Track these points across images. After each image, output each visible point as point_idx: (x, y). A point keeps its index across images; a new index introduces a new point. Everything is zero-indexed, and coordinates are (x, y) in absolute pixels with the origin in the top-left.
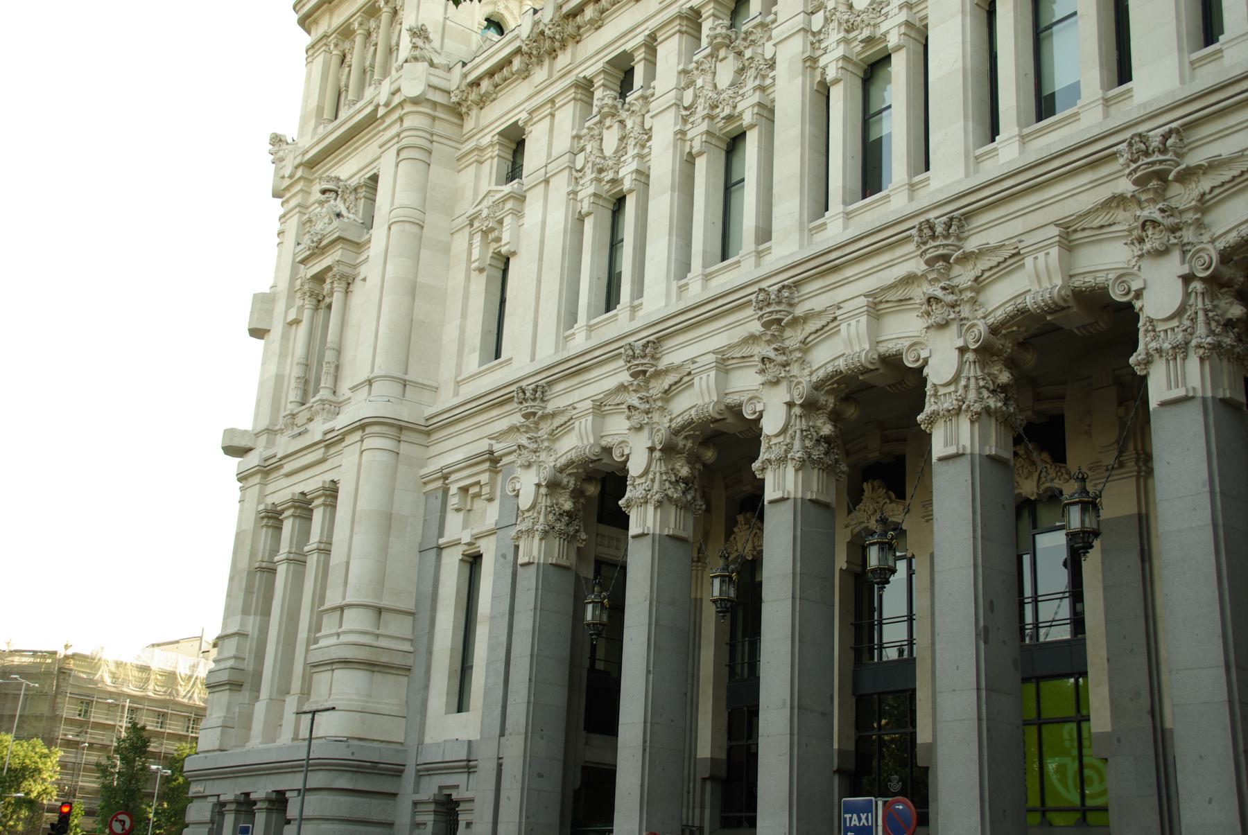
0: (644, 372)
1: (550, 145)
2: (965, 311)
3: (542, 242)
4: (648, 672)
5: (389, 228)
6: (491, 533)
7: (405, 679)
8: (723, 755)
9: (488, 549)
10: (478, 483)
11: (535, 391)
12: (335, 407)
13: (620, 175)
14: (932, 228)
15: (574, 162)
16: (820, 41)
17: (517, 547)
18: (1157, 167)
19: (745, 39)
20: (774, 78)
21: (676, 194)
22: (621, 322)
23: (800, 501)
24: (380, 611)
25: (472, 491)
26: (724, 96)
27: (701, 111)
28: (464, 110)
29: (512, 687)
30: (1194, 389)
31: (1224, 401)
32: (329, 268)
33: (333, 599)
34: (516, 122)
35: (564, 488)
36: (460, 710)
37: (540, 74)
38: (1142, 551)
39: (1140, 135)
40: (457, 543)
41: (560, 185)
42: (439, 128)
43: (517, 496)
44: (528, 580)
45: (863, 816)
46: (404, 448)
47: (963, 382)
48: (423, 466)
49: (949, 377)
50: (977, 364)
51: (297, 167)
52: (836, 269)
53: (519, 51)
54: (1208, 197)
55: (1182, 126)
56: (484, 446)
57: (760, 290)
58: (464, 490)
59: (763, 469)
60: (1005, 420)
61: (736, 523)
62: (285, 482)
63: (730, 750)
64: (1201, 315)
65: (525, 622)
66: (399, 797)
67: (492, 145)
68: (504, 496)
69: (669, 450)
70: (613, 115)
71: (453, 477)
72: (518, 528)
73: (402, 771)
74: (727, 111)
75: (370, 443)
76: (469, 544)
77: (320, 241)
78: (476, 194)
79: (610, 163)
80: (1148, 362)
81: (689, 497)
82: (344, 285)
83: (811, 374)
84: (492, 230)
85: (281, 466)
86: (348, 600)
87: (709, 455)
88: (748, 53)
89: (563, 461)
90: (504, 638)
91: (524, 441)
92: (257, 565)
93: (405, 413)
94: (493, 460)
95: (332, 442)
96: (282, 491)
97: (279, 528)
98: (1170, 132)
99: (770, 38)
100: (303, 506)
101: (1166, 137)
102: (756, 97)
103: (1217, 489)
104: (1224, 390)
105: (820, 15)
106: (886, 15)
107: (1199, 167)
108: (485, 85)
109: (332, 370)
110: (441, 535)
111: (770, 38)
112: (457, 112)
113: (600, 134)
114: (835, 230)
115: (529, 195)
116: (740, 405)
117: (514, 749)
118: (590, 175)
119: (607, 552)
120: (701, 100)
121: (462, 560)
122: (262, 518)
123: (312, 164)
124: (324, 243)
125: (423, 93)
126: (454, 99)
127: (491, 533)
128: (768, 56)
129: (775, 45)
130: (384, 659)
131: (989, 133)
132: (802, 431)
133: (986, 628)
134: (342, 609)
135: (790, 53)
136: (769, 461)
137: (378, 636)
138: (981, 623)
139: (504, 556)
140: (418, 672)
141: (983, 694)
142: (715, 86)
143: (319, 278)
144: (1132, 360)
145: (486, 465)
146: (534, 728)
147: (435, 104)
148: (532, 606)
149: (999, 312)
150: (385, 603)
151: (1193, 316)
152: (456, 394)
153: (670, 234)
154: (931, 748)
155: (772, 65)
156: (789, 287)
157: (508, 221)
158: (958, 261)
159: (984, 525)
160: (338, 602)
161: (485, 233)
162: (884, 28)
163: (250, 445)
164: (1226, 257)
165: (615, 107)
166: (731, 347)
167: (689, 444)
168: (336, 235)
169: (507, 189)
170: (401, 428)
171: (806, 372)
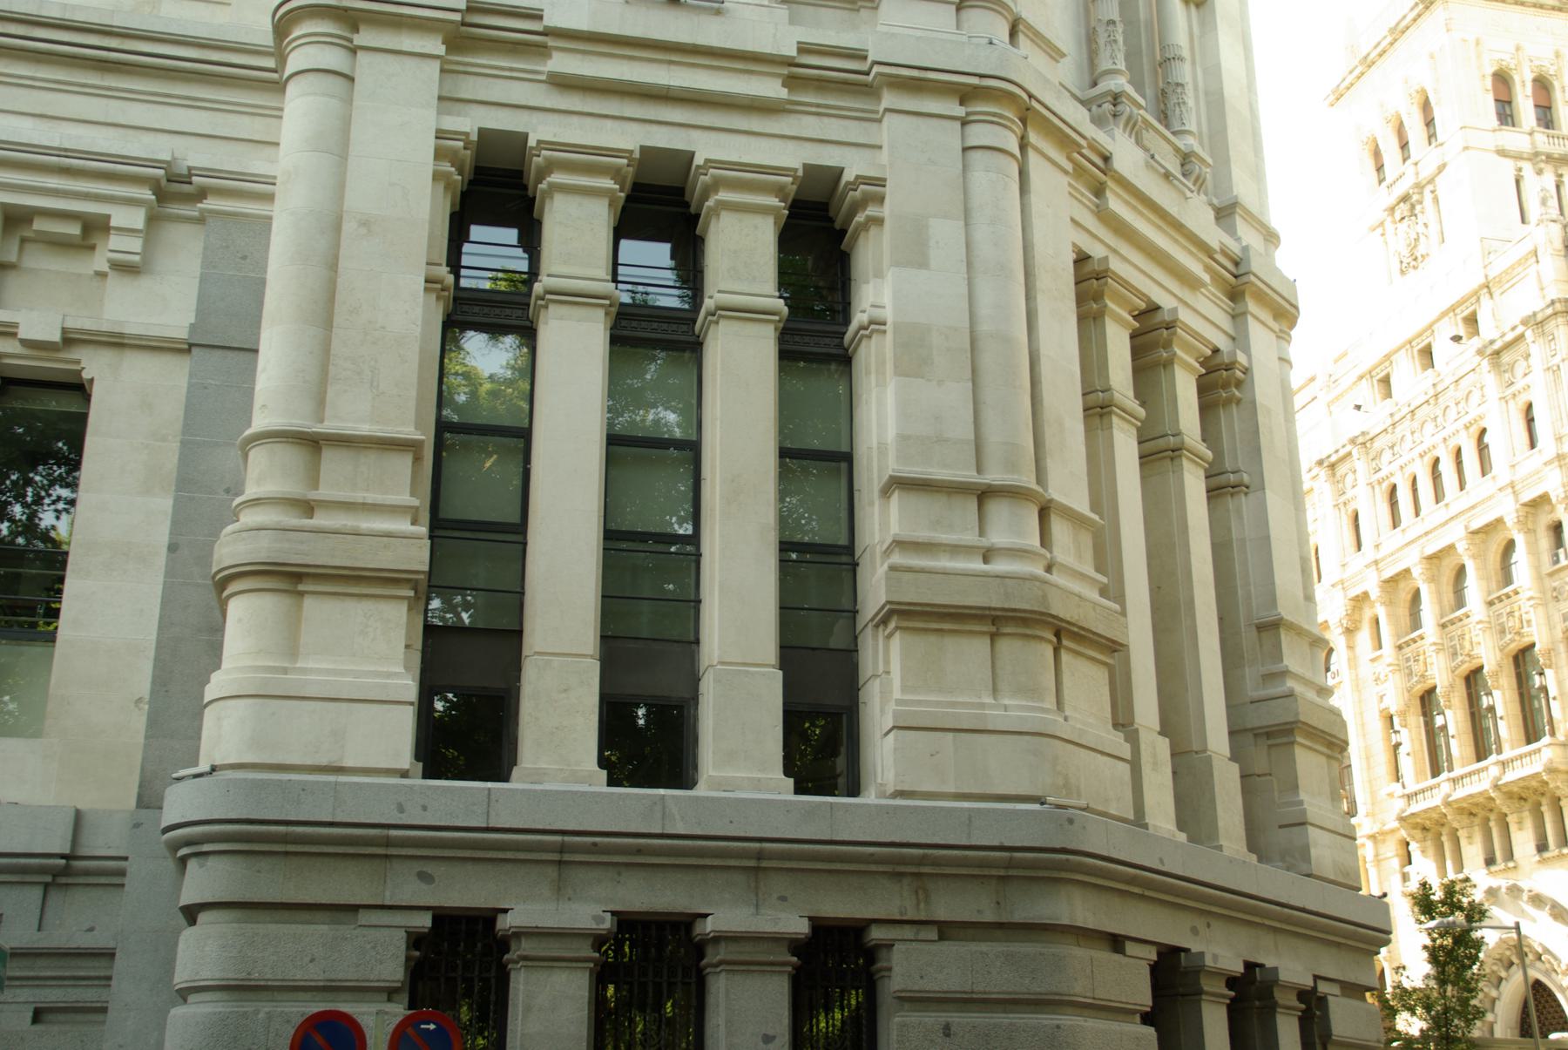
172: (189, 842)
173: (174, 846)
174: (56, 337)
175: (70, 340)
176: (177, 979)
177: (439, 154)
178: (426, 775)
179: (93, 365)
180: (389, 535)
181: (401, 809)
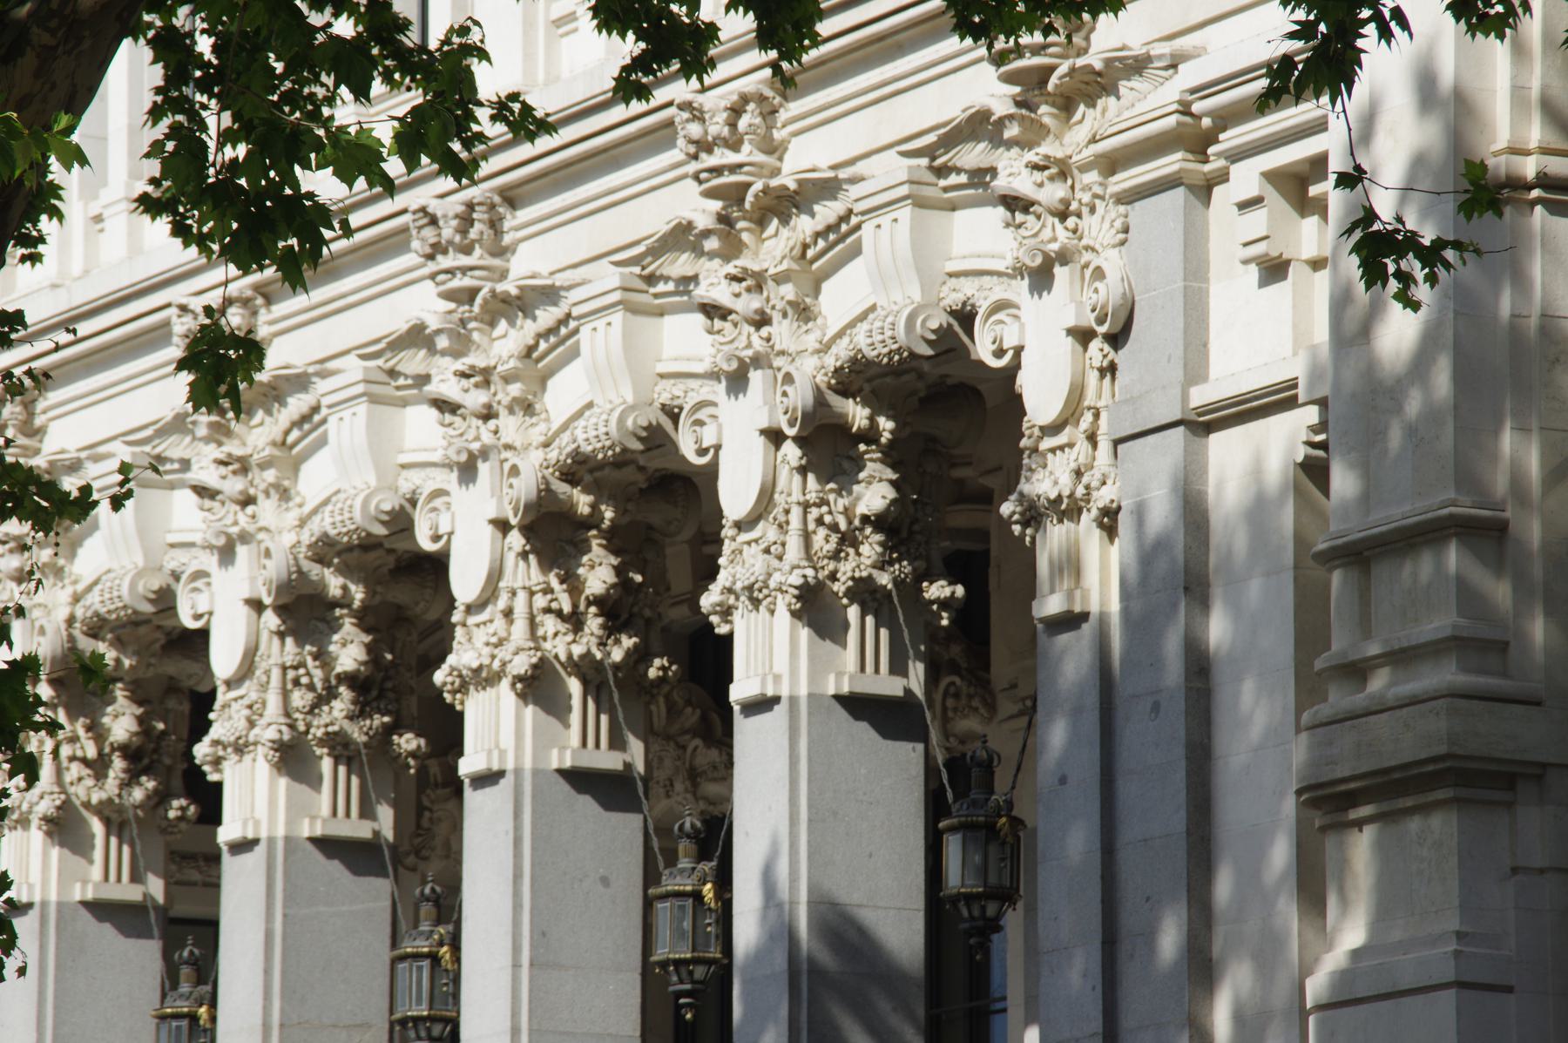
18: (728, 179)
23: (280, 845)
30: (777, 679)
50: (531, 557)
54: (810, 253)
81: (138, 794)
83: (302, 523)
98: (745, 99)
104: (839, 675)
132: (284, 669)
151: (782, 518)
171: (292, 517)
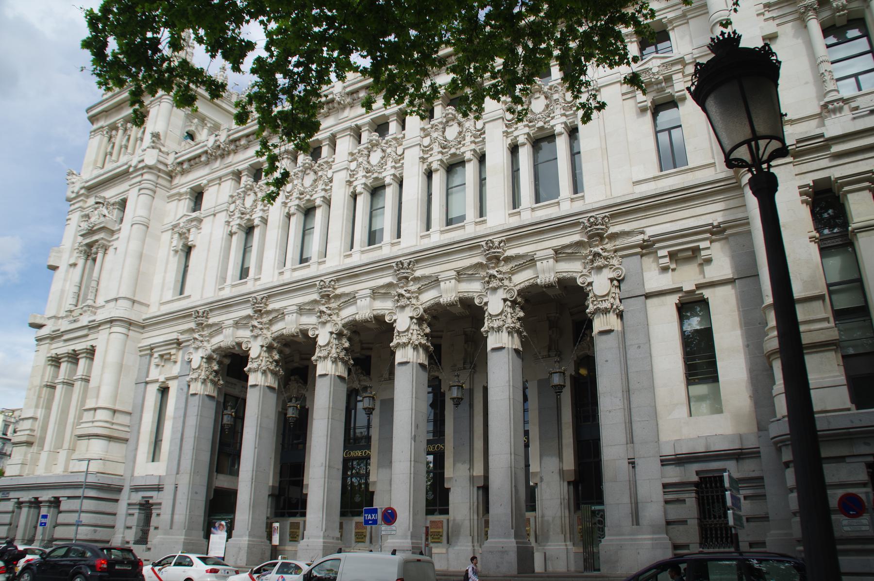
0: (260, 311)
1: (217, 197)
2: (414, 301)
3: (210, 242)
4: (255, 448)
5: (132, 226)
6: (175, 378)
7: (124, 445)
8: (277, 485)
9: (173, 386)
10: (170, 353)
11: (204, 313)
12: (93, 309)
13: (253, 217)
14: (402, 264)
15: (229, 207)
16: (354, 175)
17: (189, 386)
19: (319, 167)
20: (331, 186)
21: (280, 230)
22: (250, 286)
24: (115, 411)
25: (165, 357)
26: (307, 190)
27: (295, 194)
28: (174, 174)
29: (184, 451)
31: (515, 349)
32: (97, 241)
33: (90, 404)
34: (200, 184)
35: (214, 359)
36: (153, 461)
37: (217, 164)
38: (470, 404)
39: (491, 240)
40: (156, 381)
41: (222, 217)
42: (161, 181)
43: (191, 361)
44: (195, 402)
45: (373, 515)
46: (131, 333)
47: (411, 331)
48: (140, 343)
49: (405, 329)
51: (81, 188)
52: (356, 276)
53: (206, 152)
55: (506, 239)
56: (174, 336)
57: (322, 281)
58: (162, 356)
59: (316, 360)
60: (425, 348)
61: (290, 380)
62: (61, 344)
63: (280, 482)
64: (509, 315)
65: (192, 421)
66: (119, 502)
67: (186, 193)
68: (183, 360)
69: (270, 348)
70: (251, 190)
71: (155, 350)
72: (191, 376)
73: (122, 489)
74: (308, 197)
75: (114, 329)
76: (163, 382)
77: (93, 226)
78: (176, 215)
79: (248, 211)
80: (487, 332)
82: (103, 250)
84: (185, 233)
85: (62, 336)
86: (99, 405)
87: (287, 351)
88: (320, 173)
89: (215, 347)
90: (180, 429)
91: (196, 336)
92: (45, 383)
93: (134, 317)
94: (179, 343)
95: (94, 327)
96: (61, 348)
97: (59, 367)
99: (331, 168)
100: (74, 357)
101: (500, 243)
102: (323, 193)
103: (511, 384)
105: (355, 163)
106: (385, 169)
107: (512, 257)
108: (185, 166)
109: (94, 291)
110: (147, 376)
111: (331, 168)
112: (171, 176)
113: (244, 197)
114: (357, 258)
115: (205, 220)
116: (307, 330)
117: (184, 481)
118: (237, 215)
119: (236, 392)
120: (296, 190)
121: (158, 389)
122: (49, 360)
123: (90, 189)
124: (95, 228)
125: (155, 164)
126: (170, 169)
127: (175, 378)
128: (329, 176)
129: (333, 172)
130: (115, 434)
131: (425, 226)
133: (415, 436)
134: (95, 409)
135: (340, 178)
136: (320, 357)
137: (113, 424)
138: (413, 434)
139: (182, 389)
140: (132, 442)
141: (413, 463)
142: (303, 185)
143: (90, 245)
144: (482, 330)
145: (175, 346)
146: (195, 472)
147: (160, 170)
148: (196, 414)
149: (428, 303)
150: (117, 407)
152: (159, 310)
153: (276, 248)
154: (374, 483)
155: (331, 181)
156: (334, 281)
157: (193, 230)
158: (412, 280)
159: (416, 392)
160: (93, 406)
161: (180, 235)
162: (384, 174)
163: (44, 323)
164: (520, 292)
165: (252, 186)
166: (305, 304)
167: (279, 345)
168: (102, 226)
169: (194, 215)
170: (130, 324)
172: (781, 441)
173: (776, 443)
174: (694, 288)
175: (699, 287)
176: (788, 485)
177: (801, 194)
178: (858, 408)
179: (707, 293)
180: (822, 329)
181: (852, 422)
